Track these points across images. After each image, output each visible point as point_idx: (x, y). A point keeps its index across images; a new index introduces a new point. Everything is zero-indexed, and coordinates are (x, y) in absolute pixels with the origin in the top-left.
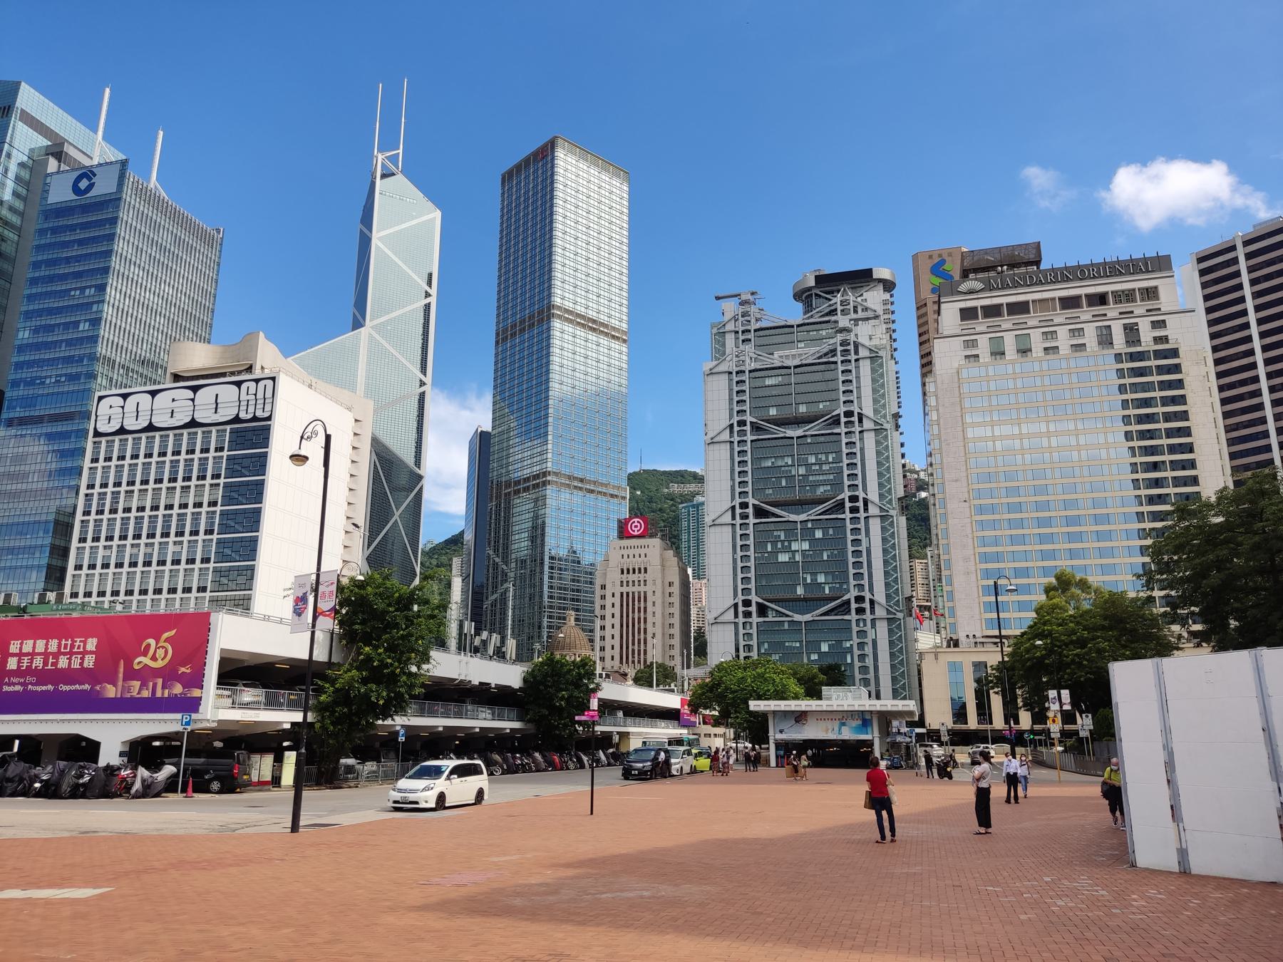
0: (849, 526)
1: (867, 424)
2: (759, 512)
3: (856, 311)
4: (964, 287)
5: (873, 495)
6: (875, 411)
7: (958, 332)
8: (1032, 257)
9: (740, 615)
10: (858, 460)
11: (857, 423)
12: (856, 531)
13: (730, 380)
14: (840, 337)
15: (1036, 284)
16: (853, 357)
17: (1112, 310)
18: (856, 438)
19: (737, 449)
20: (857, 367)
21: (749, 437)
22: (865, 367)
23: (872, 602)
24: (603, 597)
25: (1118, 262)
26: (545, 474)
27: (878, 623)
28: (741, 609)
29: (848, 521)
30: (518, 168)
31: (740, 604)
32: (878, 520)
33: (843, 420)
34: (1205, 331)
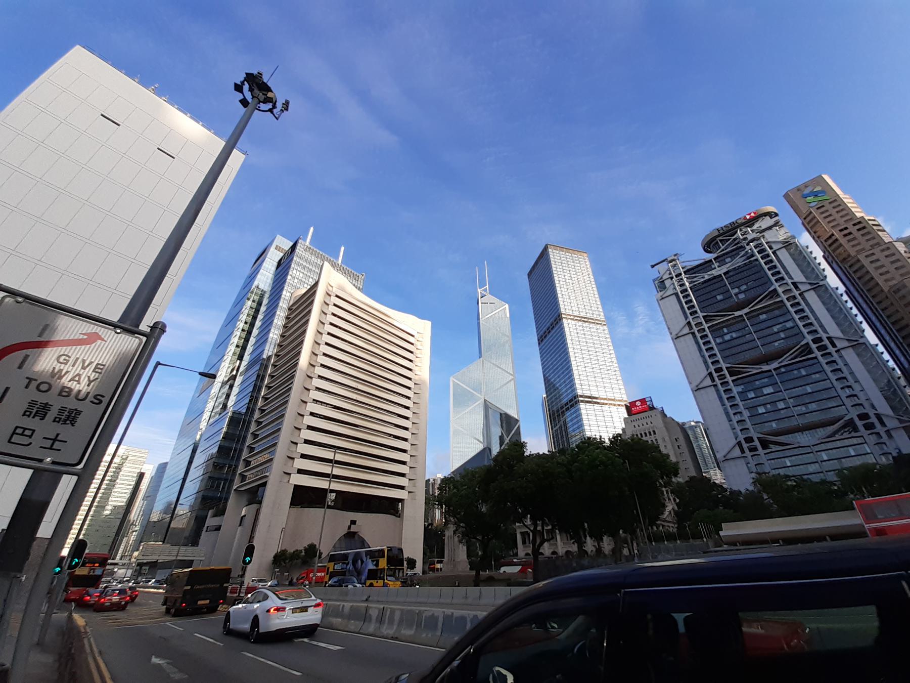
1: (803, 288)
9: (747, 451)
22: (784, 255)
23: (878, 416)
26: (575, 398)
28: (745, 445)
29: (820, 358)
30: (534, 267)
33: (780, 290)
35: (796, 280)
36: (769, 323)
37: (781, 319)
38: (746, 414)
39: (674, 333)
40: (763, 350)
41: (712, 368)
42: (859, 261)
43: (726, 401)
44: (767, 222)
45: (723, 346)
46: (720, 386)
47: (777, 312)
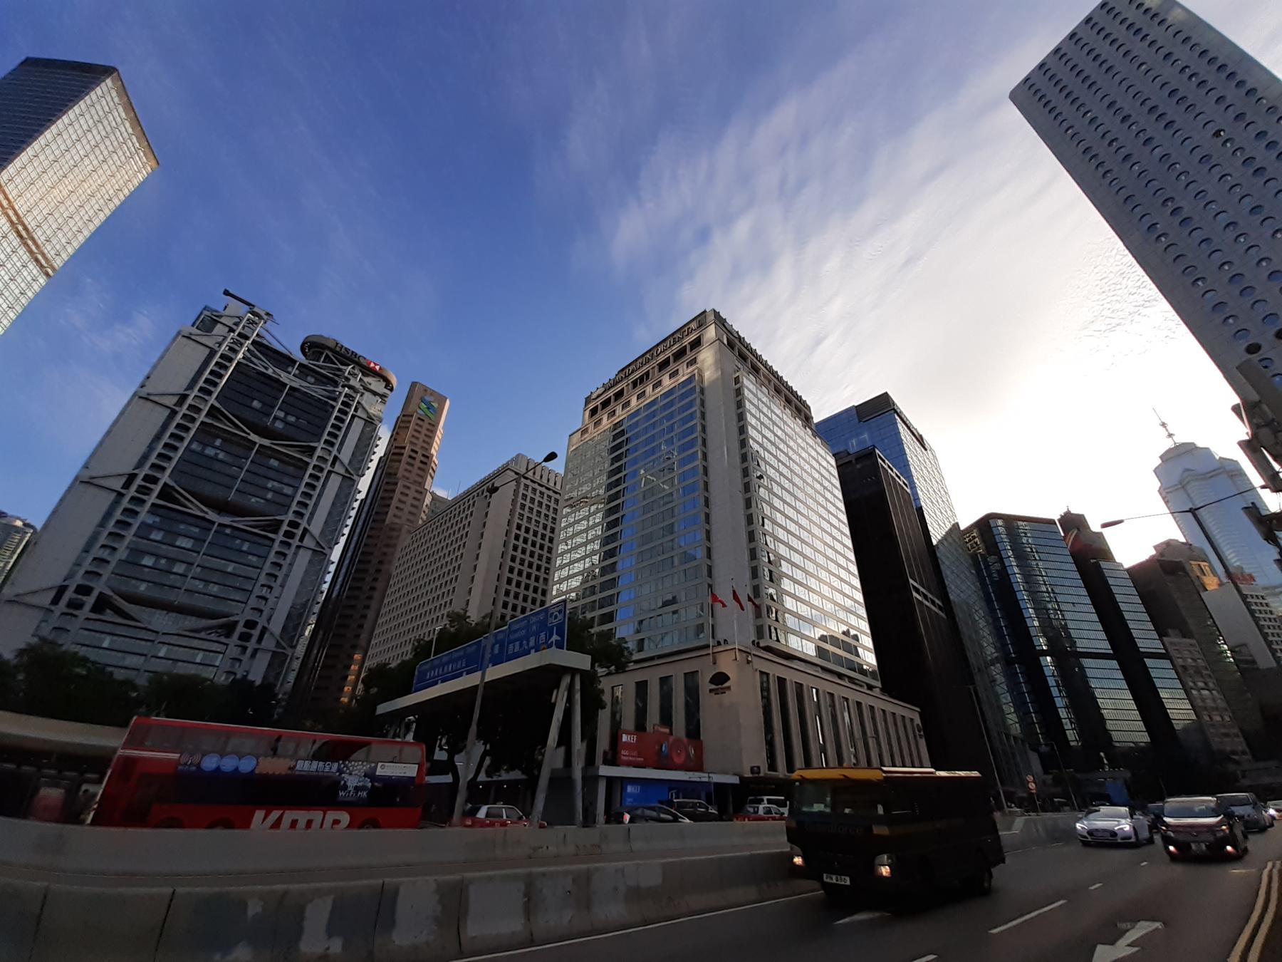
0: (276, 547)
1: (338, 468)
18: (323, 475)
21: (202, 417)
22: (358, 426)
28: (69, 595)
31: (72, 588)
33: (318, 452)
35: (340, 456)
36: (271, 474)
37: (286, 480)
38: (122, 553)
40: (232, 496)
43: (112, 522)
44: (378, 386)
47: (291, 469)
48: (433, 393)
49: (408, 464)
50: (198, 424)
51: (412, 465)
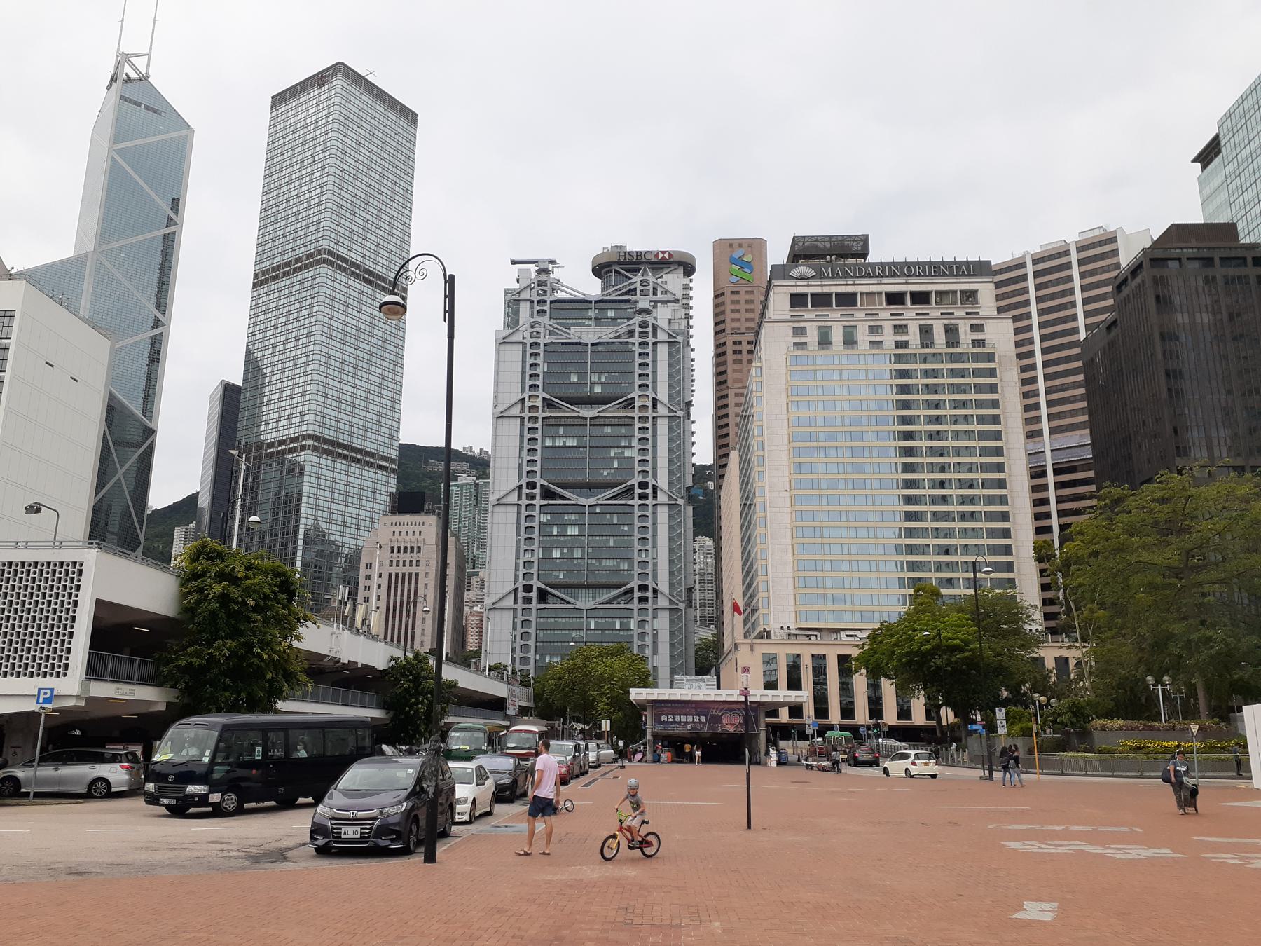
0: (637, 512)
1: (662, 410)
2: (547, 494)
3: (655, 294)
4: (795, 272)
5: (663, 483)
6: (670, 397)
7: (788, 317)
8: (857, 248)
9: (520, 601)
10: (649, 446)
11: (650, 408)
12: (643, 517)
13: (524, 352)
14: (637, 319)
15: (865, 277)
16: (650, 340)
17: (933, 310)
19: (528, 425)
20: (655, 350)
21: (540, 414)
23: (655, 591)
24: (368, 577)
25: (943, 263)
27: (660, 614)
28: (521, 594)
29: (636, 507)
31: (521, 589)
32: (666, 509)
33: (637, 404)
34: (1012, 339)
36: (608, 442)
39: (501, 408)
40: (587, 477)
41: (524, 482)
42: (726, 396)
45: (548, 454)
46: (523, 507)
47: (623, 431)
48: (740, 243)
49: (735, 362)
50: (540, 420)
51: (740, 362)
